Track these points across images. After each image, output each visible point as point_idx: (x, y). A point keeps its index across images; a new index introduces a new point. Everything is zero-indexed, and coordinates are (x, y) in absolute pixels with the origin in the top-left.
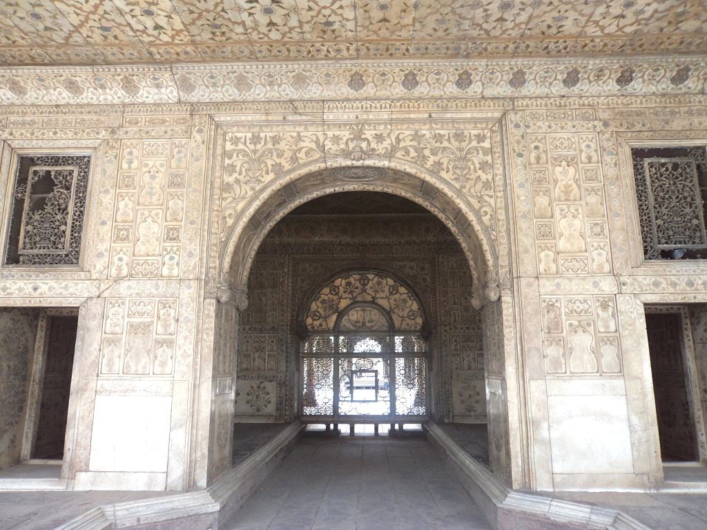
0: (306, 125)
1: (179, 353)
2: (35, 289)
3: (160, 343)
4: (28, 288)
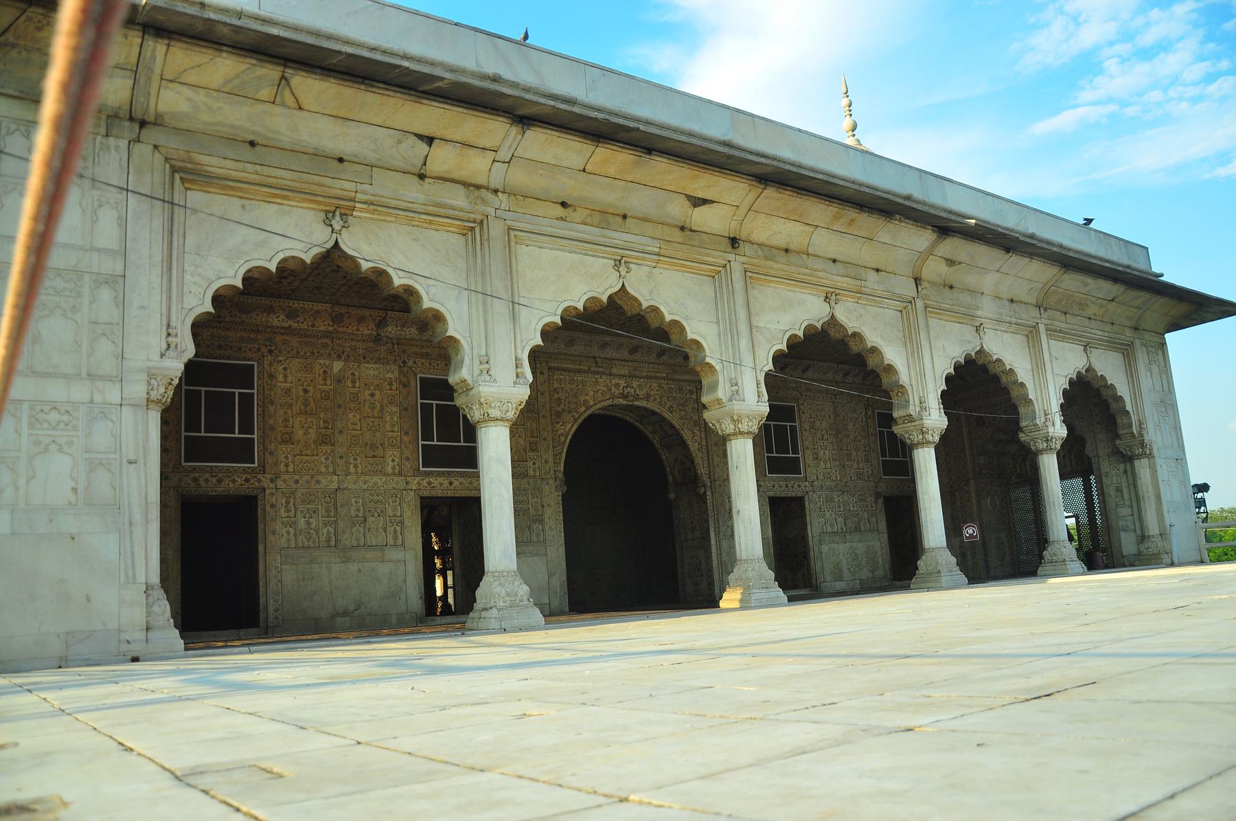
0: (602, 374)
1: (547, 527)
2: (451, 484)
3: (535, 521)
4: (446, 484)
